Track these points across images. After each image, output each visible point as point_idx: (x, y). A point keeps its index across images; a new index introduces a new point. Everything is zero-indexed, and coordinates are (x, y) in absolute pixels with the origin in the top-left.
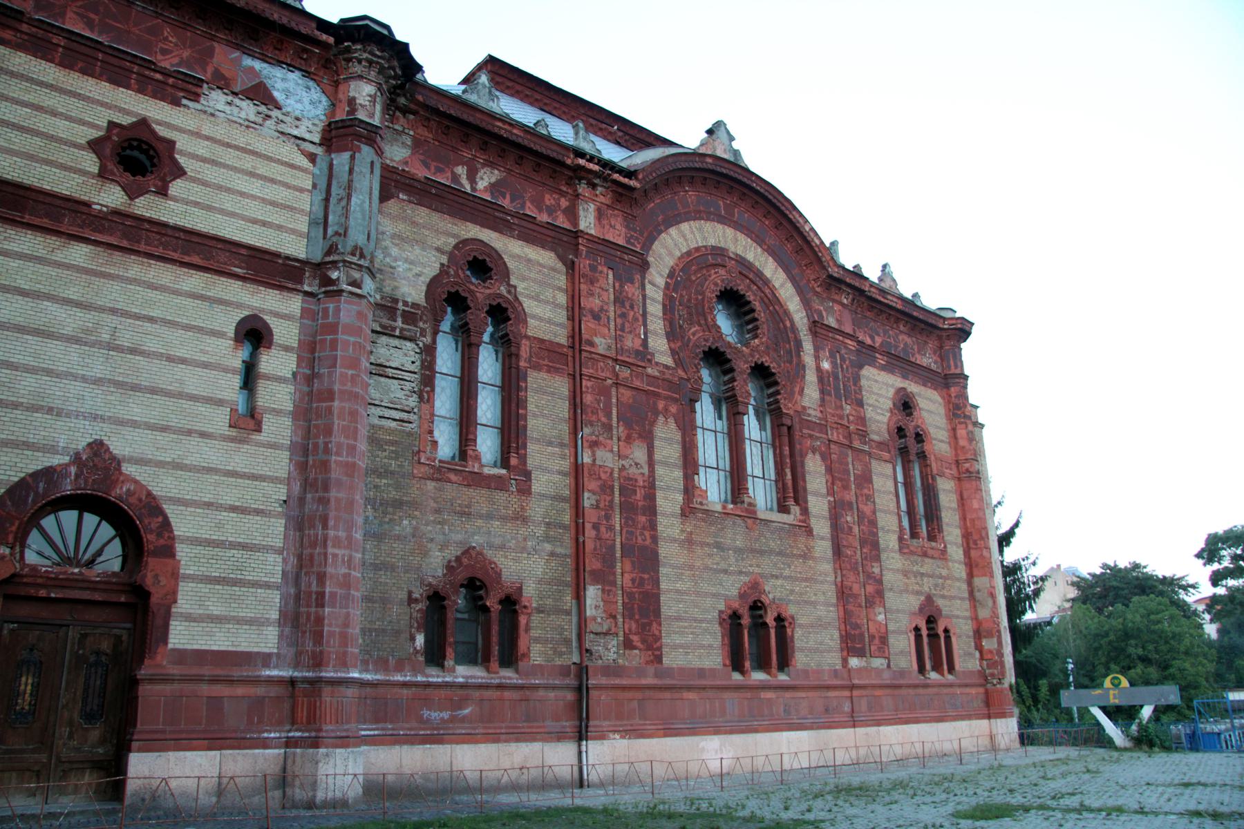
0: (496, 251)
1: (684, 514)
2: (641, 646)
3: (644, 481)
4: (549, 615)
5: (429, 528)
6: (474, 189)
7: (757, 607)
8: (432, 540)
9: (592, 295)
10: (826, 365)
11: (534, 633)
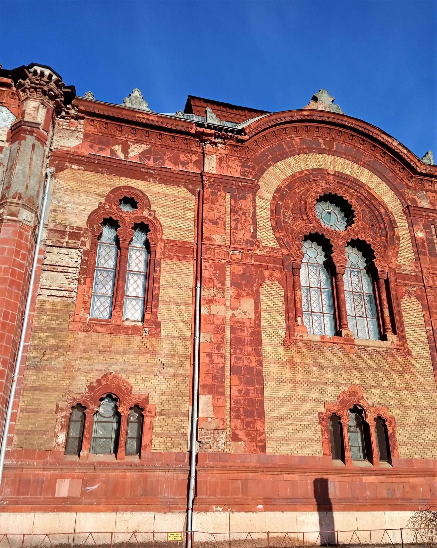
0: (141, 192)
1: (285, 343)
2: (246, 439)
3: (251, 323)
4: (169, 417)
5: (78, 362)
6: (126, 157)
8: (79, 369)
9: (213, 210)
10: (420, 235)
11: (155, 430)
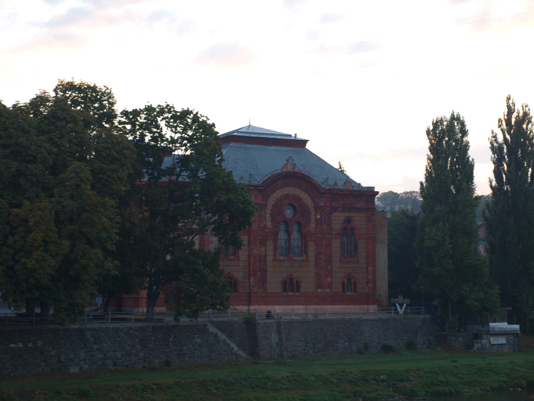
7: (291, 279)
